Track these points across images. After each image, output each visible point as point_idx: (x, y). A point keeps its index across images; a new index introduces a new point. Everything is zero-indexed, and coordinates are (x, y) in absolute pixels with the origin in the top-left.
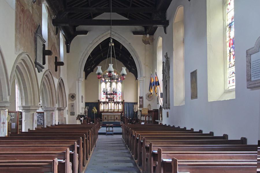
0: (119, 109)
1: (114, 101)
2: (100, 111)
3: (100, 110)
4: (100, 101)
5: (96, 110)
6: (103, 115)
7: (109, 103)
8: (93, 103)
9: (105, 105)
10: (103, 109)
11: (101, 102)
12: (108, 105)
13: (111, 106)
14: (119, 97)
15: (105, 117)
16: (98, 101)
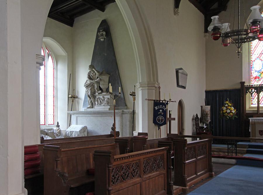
0: (258, 107)
2: (247, 112)
3: (247, 108)
4: (246, 84)
5: (233, 108)
6: (254, 124)
8: (226, 91)
9: (256, 93)
10: (256, 105)
11: (252, 87)
15: (258, 129)
16: (239, 87)
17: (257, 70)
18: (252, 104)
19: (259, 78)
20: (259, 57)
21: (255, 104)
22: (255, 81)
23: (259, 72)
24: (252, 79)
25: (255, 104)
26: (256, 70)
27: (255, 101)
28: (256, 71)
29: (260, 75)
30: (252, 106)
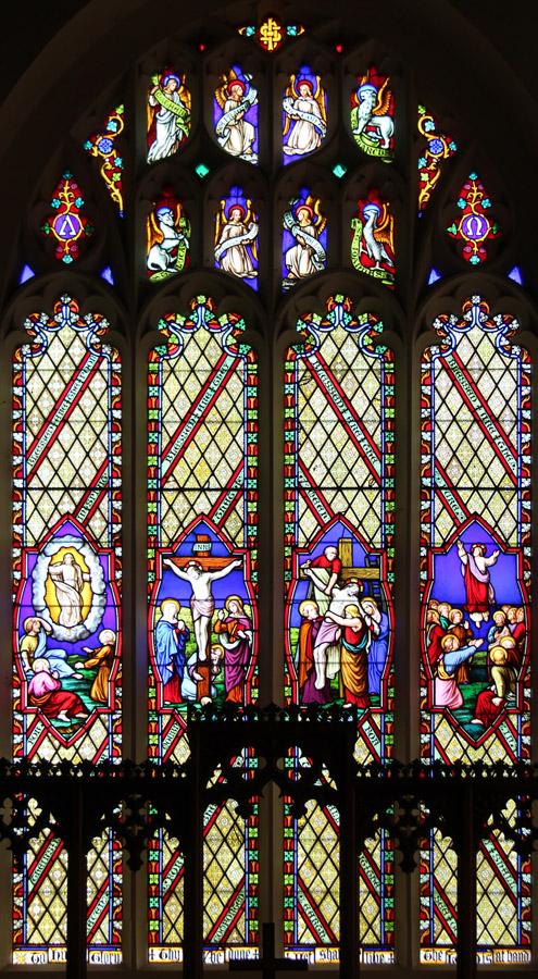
1: (343, 764)
7: (224, 821)
10: (59, 956)
12: (194, 875)
13: (270, 895)
14: (474, 671)
17: (62, 633)
18: (23, 944)
19: (78, 705)
20: (81, 518)
21: (46, 945)
22: (48, 729)
23: (76, 649)
24: (23, 712)
25: (46, 945)
26: (51, 636)
27: (46, 919)
28: (53, 642)
29: (89, 682)
30: (21, 958)
